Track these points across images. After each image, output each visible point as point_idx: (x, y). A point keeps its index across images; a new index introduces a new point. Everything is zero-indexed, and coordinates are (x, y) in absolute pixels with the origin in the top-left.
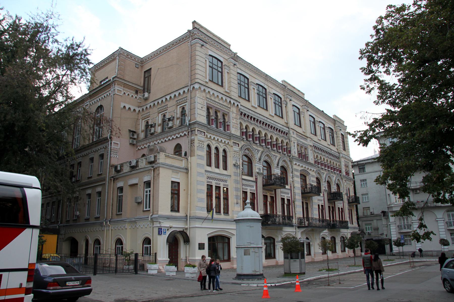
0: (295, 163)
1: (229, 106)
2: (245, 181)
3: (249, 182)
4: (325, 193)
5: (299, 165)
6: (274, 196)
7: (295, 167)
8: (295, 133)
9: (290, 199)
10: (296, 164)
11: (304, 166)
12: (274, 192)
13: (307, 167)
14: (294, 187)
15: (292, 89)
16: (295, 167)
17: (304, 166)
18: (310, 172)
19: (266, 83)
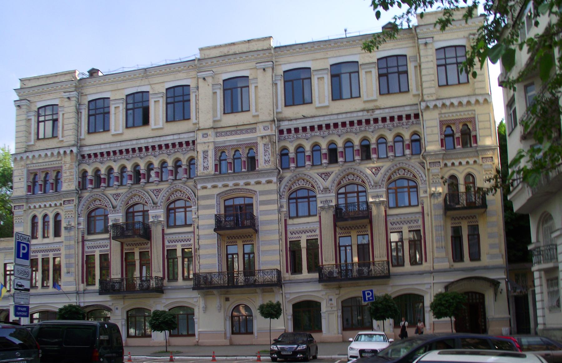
0: (199, 186)
1: (60, 159)
2: (90, 243)
3: (98, 242)
4: (323, 214)
5: (215, 187)
6: (149, 250)
7: (201, 193)
8: (210, 132)
9: (193, 247)
10: (205, 188)
11: (231, 183)
12: (149, 245)
13: (242, 182)
14: (198, 228)
15: (225, 51)
16: (201, 193)
17: (231, 183)
18: (257, 188)
19: (145, 81)
